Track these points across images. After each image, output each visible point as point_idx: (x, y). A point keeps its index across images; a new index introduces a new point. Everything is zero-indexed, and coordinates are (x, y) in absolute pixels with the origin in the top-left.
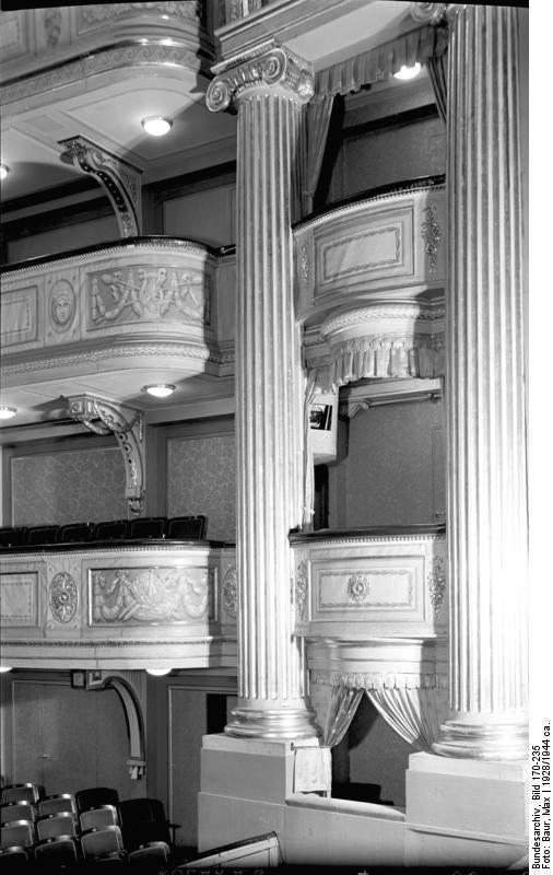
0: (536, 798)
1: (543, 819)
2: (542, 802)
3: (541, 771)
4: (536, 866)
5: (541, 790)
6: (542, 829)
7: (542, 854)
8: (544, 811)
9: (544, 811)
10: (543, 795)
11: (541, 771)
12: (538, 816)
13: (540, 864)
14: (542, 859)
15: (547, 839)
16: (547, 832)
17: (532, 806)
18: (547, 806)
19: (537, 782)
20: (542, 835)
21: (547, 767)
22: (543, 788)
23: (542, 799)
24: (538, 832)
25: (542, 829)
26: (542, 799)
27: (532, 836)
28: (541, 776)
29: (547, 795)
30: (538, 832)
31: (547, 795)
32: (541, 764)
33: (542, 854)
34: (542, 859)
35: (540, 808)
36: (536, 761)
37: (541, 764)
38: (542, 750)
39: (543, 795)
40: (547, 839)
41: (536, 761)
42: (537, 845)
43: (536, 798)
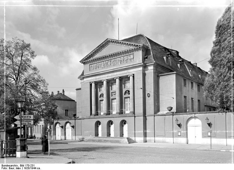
0: (21, 166)
1: (15, 167)
2: (20, 167)
3: (28, 167)
4: (2, 165)
5: (23, 167)
6: (12, 167)
7: (6, 167)
8: (17, 168)
9: (17, 168)
10: (21, 167)
11: (28, 167)
12: (16, 166)
13: (3, 167)
14: (4, 167)
15: (10, 168)
17: (19, 165)
18: (18, 168)
19: (25, 166)
20: (11, 167)
21: (29, 168)
22: (23, 167)
24: (11, 166)
25: (12, 167)
27: (10, 164)
29: (21, 168)
30: (11, 166)
31: (21, 168)
32: (30, 167)
33: (6, 167)
34: (4, 167)
36: (31, 165)
37: (30, 167)
40: (10, 168)
41: (31, 165)
42: (8, 166)
43: (21, 166)
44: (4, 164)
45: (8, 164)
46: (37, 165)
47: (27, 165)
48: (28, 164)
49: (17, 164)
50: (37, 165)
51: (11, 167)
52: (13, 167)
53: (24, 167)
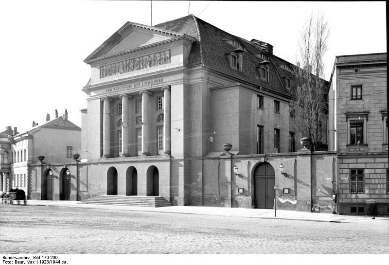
0: (34, 258)
1: (25, 261)
2: (32, 260)
3: (46, 259)
4: (4, 257)
5: (38, 260)
6: (21, 260)
7: (9, 260)
8: (28, 261)
9: (28, 261)
10: (35, 260)
11: (46, 259)
12: (26, 258)
13: (5, 259)
14: (7, 260)
15: (16, 262)
16: (19, 263)
17: (31, 256)
18: (31, 262)
19: (41, 259)
20: (18, 260)
21: (48, 262)
22: (39, 260)
23: (34, 260)
24: (19, 258)
25: (21, 260)
26: (34, 260)
27: (17, 256)
28: (44, 260)
29: (36, 262)
30: (19, 258)
31: (36, 262)
32: (49, 260)
33: (9, 260)
34: (7, 260)
35: (30, 259)
36: (51, 258)
37: (49, 260)
38: (56, 260)
39: (35, 260)
40: (16, 262)
41: (51, 258)
42: (14, 258)
43: (34, 258)
44: (6, 256)
45: (14, 256)
46: (61, 258)
47: (44, 257)
48: (47, 255)
49: (28, 256)
50: (61, 258)
51: (18, 260)
52: (22, 260)
53: (40, 260)
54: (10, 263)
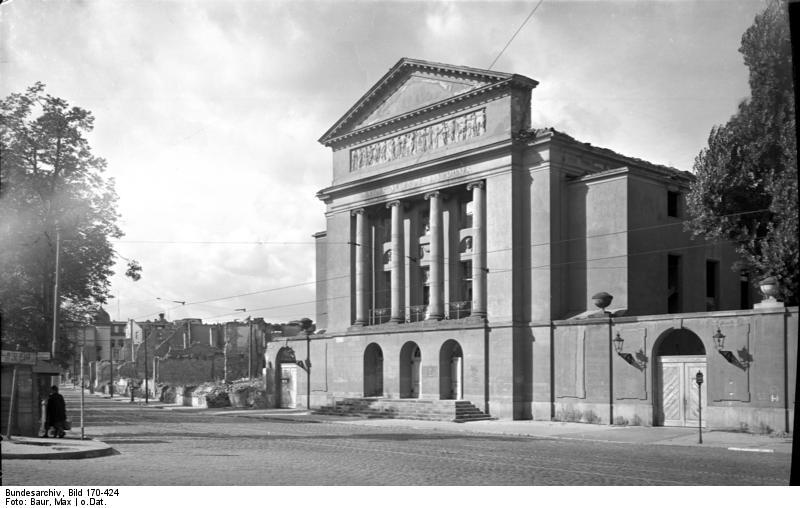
0: (71, 493)
1: (51, 499)
2: (67, 498)
4: (8, 492)
6: (42, 498)
7: (19, 498)
8: (59, 500)
9: (59, 500)
10: (73, 498)
12: (54, 494)
13: (10, 497)
14: (14, 498)
15: (33, 502)
16: (39, 503)
18: (63, 502)
22: (80, 499)
24: (39, 494)
25: (42, 498)
29: (73, 502)
30: (39, 494)
31: (73, 502)
33: (19, 498)
34: (14, 498)
35: (61, 496)
39: (73, 499)
40: (33, 502)
42: (28, 493)
43: (71, 493)
51: (39, 498)
52: (46, 498)
54: (21, 503)
